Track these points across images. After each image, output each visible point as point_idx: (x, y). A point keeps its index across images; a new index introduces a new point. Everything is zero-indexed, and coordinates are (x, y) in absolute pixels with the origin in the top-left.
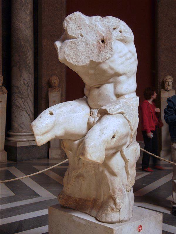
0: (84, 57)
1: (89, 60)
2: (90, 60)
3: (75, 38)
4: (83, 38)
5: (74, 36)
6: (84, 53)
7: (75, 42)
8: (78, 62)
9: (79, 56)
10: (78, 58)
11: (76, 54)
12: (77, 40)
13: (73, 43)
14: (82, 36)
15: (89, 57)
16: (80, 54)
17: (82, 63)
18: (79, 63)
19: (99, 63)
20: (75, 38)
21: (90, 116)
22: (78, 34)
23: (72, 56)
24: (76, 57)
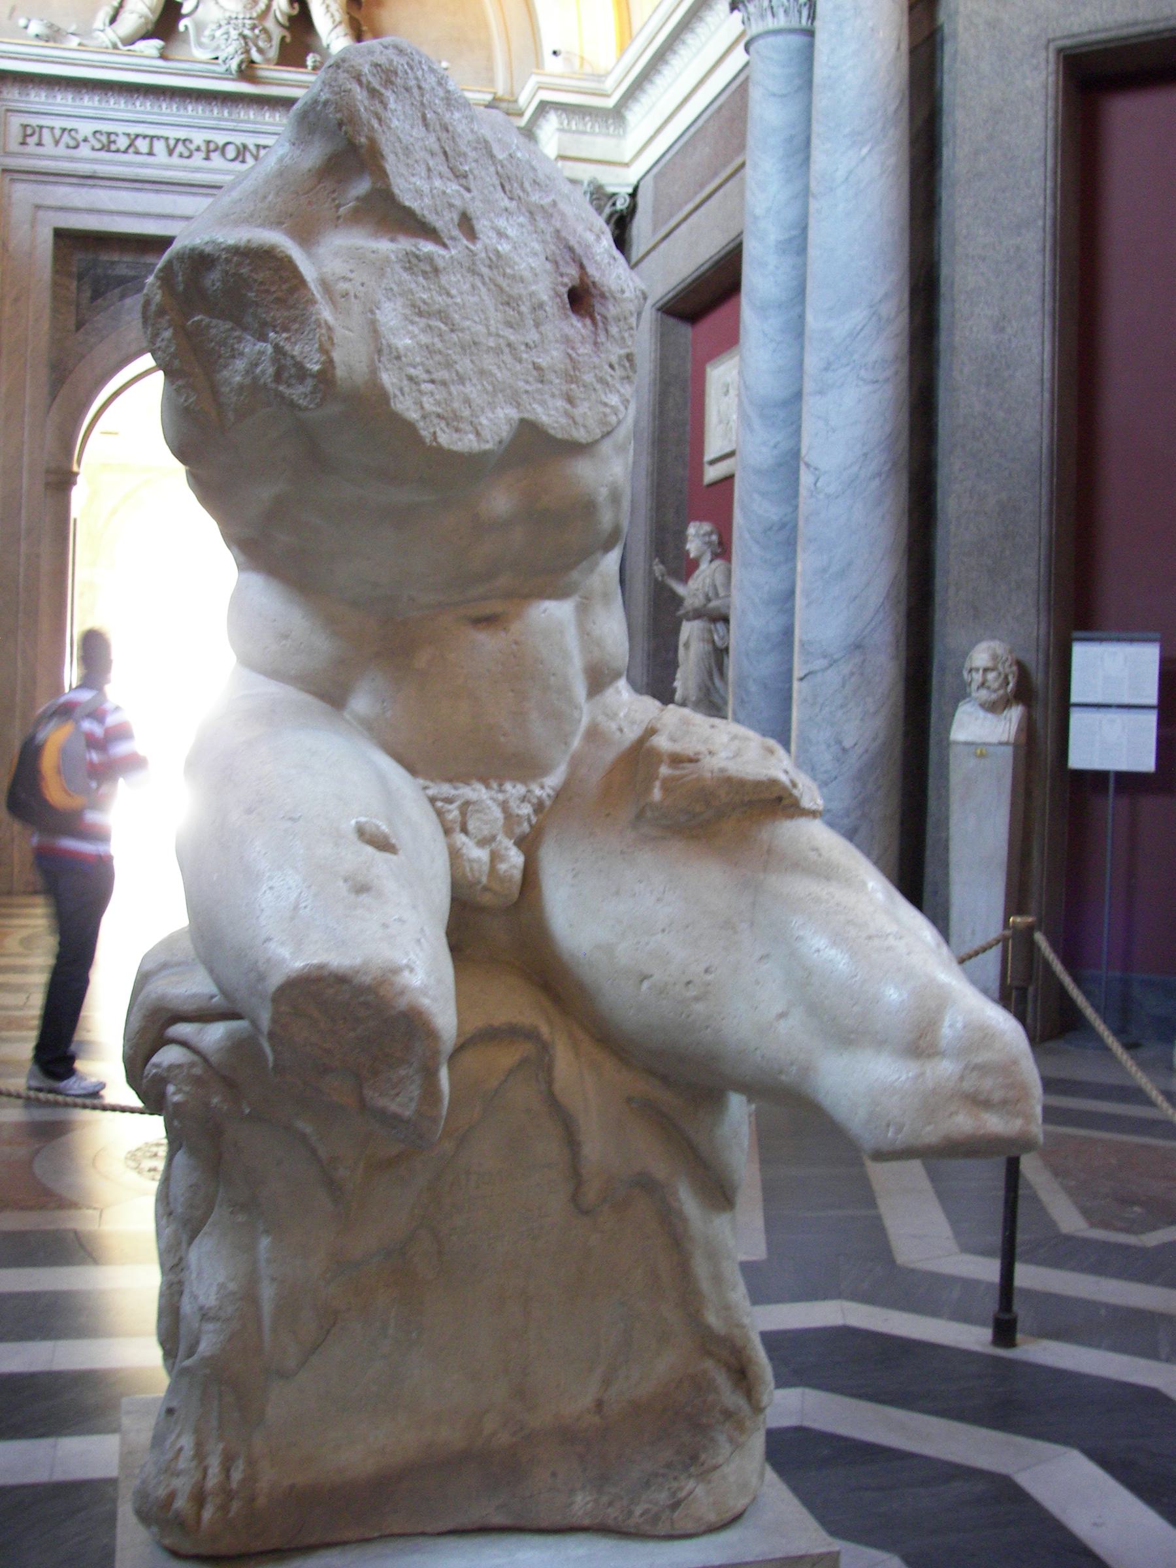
0: (490, 388)
1: (514, 413)
2: (523, 421)
3: (429, 232)
4: (478, 247)
5: (431, 218)
6: (488, 362)
7: (441, 264)
8: (452, 420)
9: (461, 380)
10: (452, 388)
11: (449, 365)
12: (442, 252)
13: (424, 273)
14: (466, 224)
15: (515, 399)
16: (464, 365)
17: (478, 434)
18: (457, 430)
19: (576, 449)
20: (429, 232)
21: (447, 832)
22: (451, 206)
23: (418, 372)
24: (444, 383)
